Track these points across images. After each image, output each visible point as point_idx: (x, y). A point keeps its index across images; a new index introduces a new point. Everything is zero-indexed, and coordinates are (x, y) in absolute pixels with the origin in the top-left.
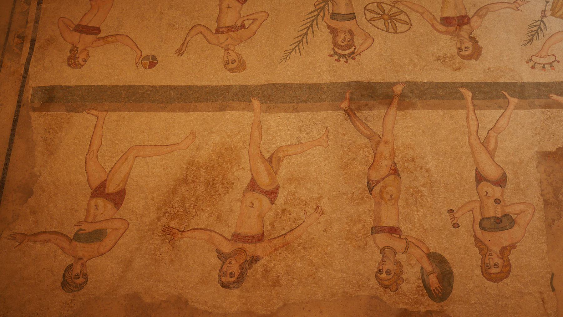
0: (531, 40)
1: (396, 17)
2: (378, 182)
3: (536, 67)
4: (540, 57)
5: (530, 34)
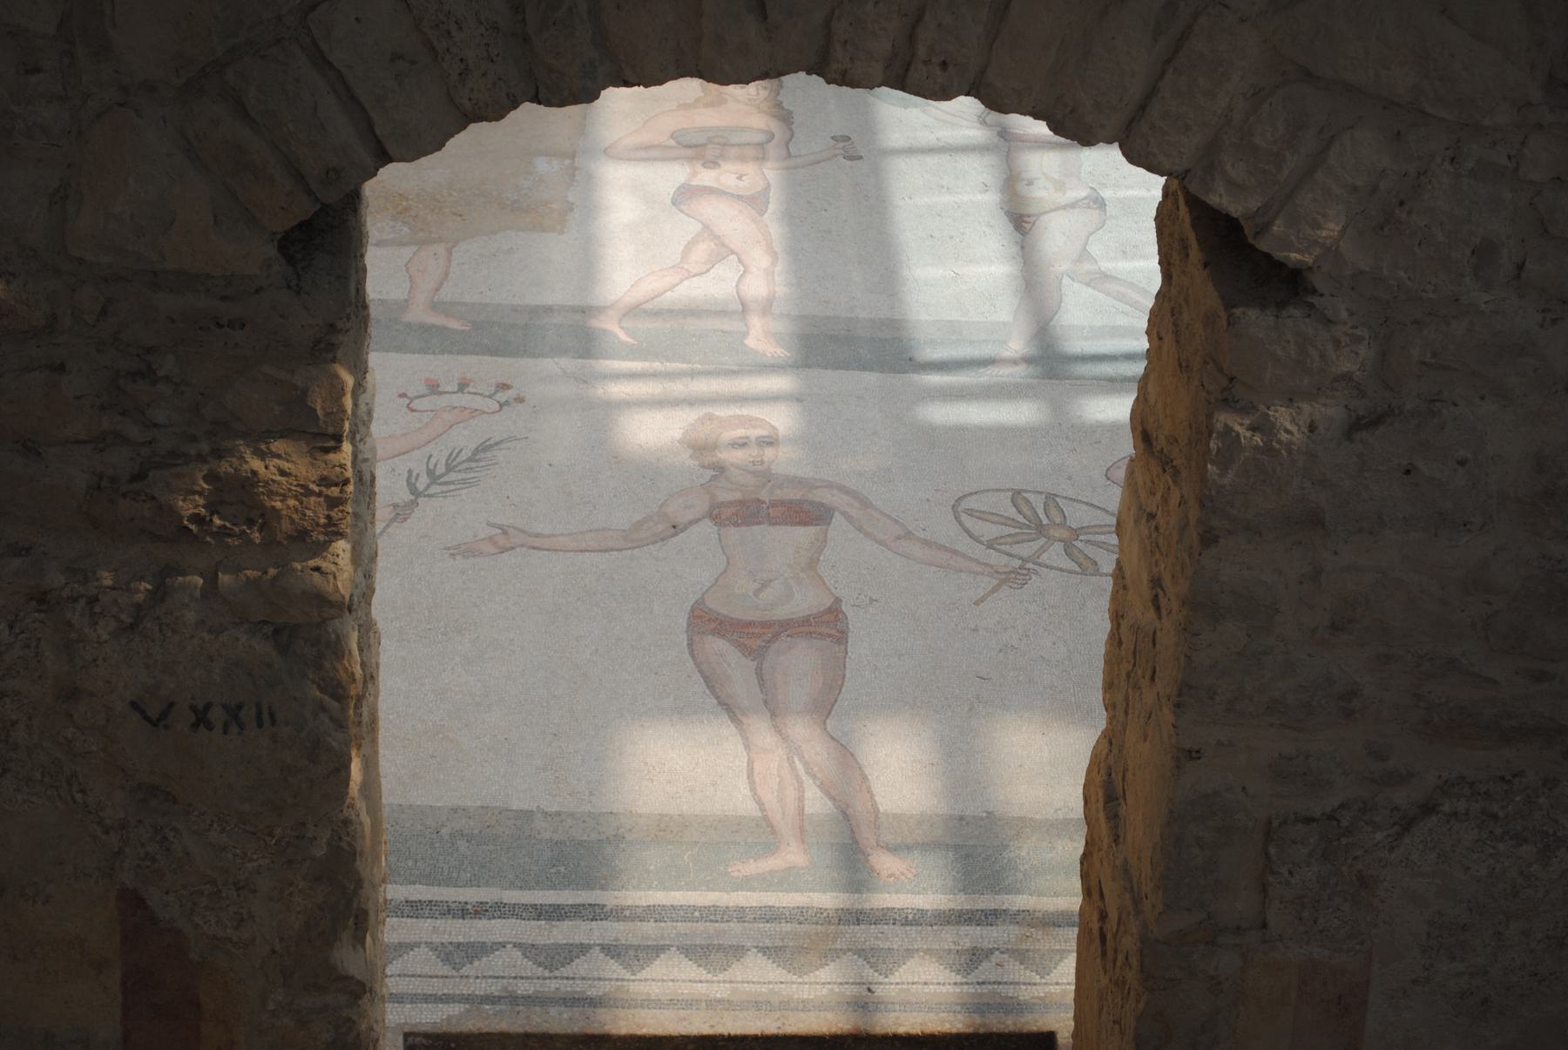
0: (484, 448)
1: (1017, 530)
2: (1073, 205)
3: (493, 388)
4: (466, 408)
5: (481, 464)
